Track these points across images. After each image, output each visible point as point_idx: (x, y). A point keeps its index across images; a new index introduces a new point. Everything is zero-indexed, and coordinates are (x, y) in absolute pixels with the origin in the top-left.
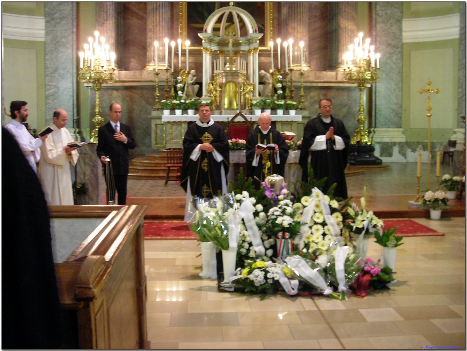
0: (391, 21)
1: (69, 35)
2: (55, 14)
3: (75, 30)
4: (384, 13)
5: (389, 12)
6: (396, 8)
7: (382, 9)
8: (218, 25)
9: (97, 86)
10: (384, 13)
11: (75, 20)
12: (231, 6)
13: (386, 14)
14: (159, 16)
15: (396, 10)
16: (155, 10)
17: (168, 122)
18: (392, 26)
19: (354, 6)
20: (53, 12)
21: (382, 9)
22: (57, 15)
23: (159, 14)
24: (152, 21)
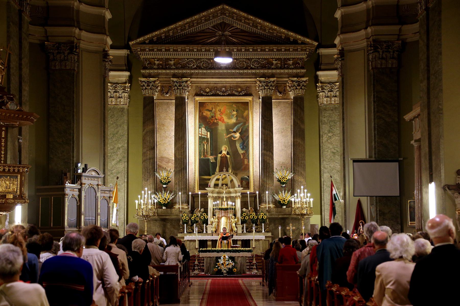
0: (333, 172)
1: (122, 184)
2: (113, 170)
3: (126, 180)
4: (328, 166)
5: (332, 166)
6: (336, 163)
7: (327, 163)
8: (217, 182)
9: (146, 219)
10: (328, 166)
11: (126, 174)
12: (224, 172)
13: (330, 167)
14: (182, 175)
15: (337, 164)
16: (179, 172)
17: (188, 240)
18: (334, 175)
19: (303, 166)
20: (112, 169)
21: (327, 163)
22: (114, 171)
23: (182, 174)
24: (177, 178)
